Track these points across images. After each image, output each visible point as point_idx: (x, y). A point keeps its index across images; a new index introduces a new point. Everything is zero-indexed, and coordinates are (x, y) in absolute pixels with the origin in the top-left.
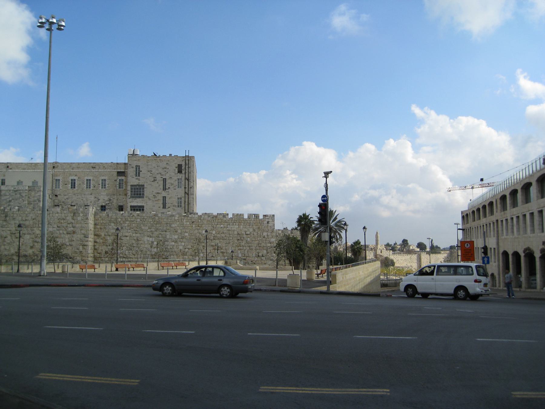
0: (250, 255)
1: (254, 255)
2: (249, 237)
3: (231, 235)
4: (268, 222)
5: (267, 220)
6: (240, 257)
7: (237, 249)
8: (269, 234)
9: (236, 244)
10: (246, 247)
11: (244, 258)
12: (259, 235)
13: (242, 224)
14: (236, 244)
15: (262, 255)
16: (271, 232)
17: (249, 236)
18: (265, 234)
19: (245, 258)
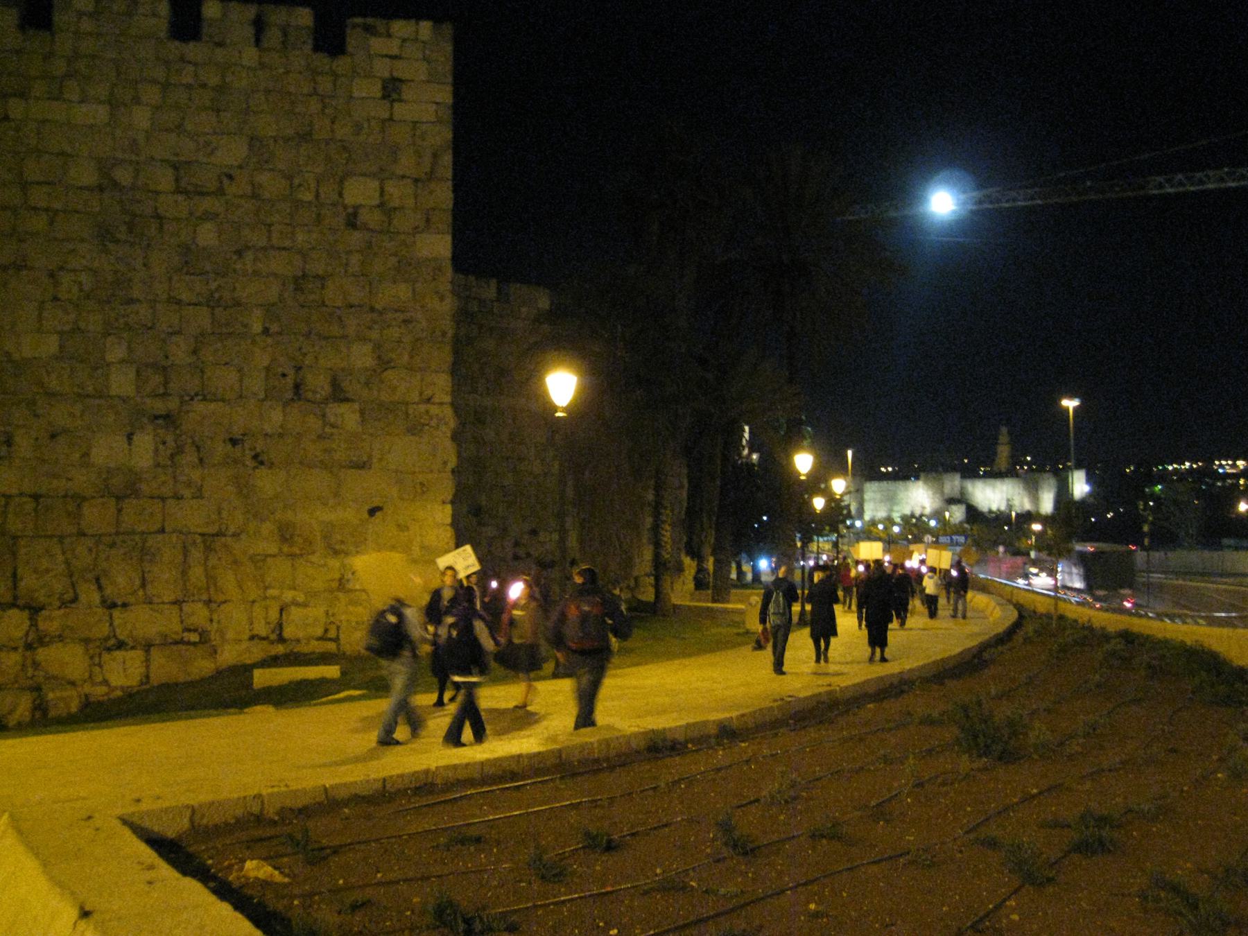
0: (223, 379)
1: (256, 384)
2: (207, 216)
3: (39, 197)
4: (392, 89)
5: (382, 69)
6: (124, 400)
7: (94, 323)
8: (398, 192)
9: (83, 277)
10: (179, 302)
11: (159, 406)
12: (308, 197)
13: (151, 94)
14: (83, 277)
15: (335, 384)
16: (416, 181)
17: (207, 204)
18: (360, 192)
19: (173, 404)
